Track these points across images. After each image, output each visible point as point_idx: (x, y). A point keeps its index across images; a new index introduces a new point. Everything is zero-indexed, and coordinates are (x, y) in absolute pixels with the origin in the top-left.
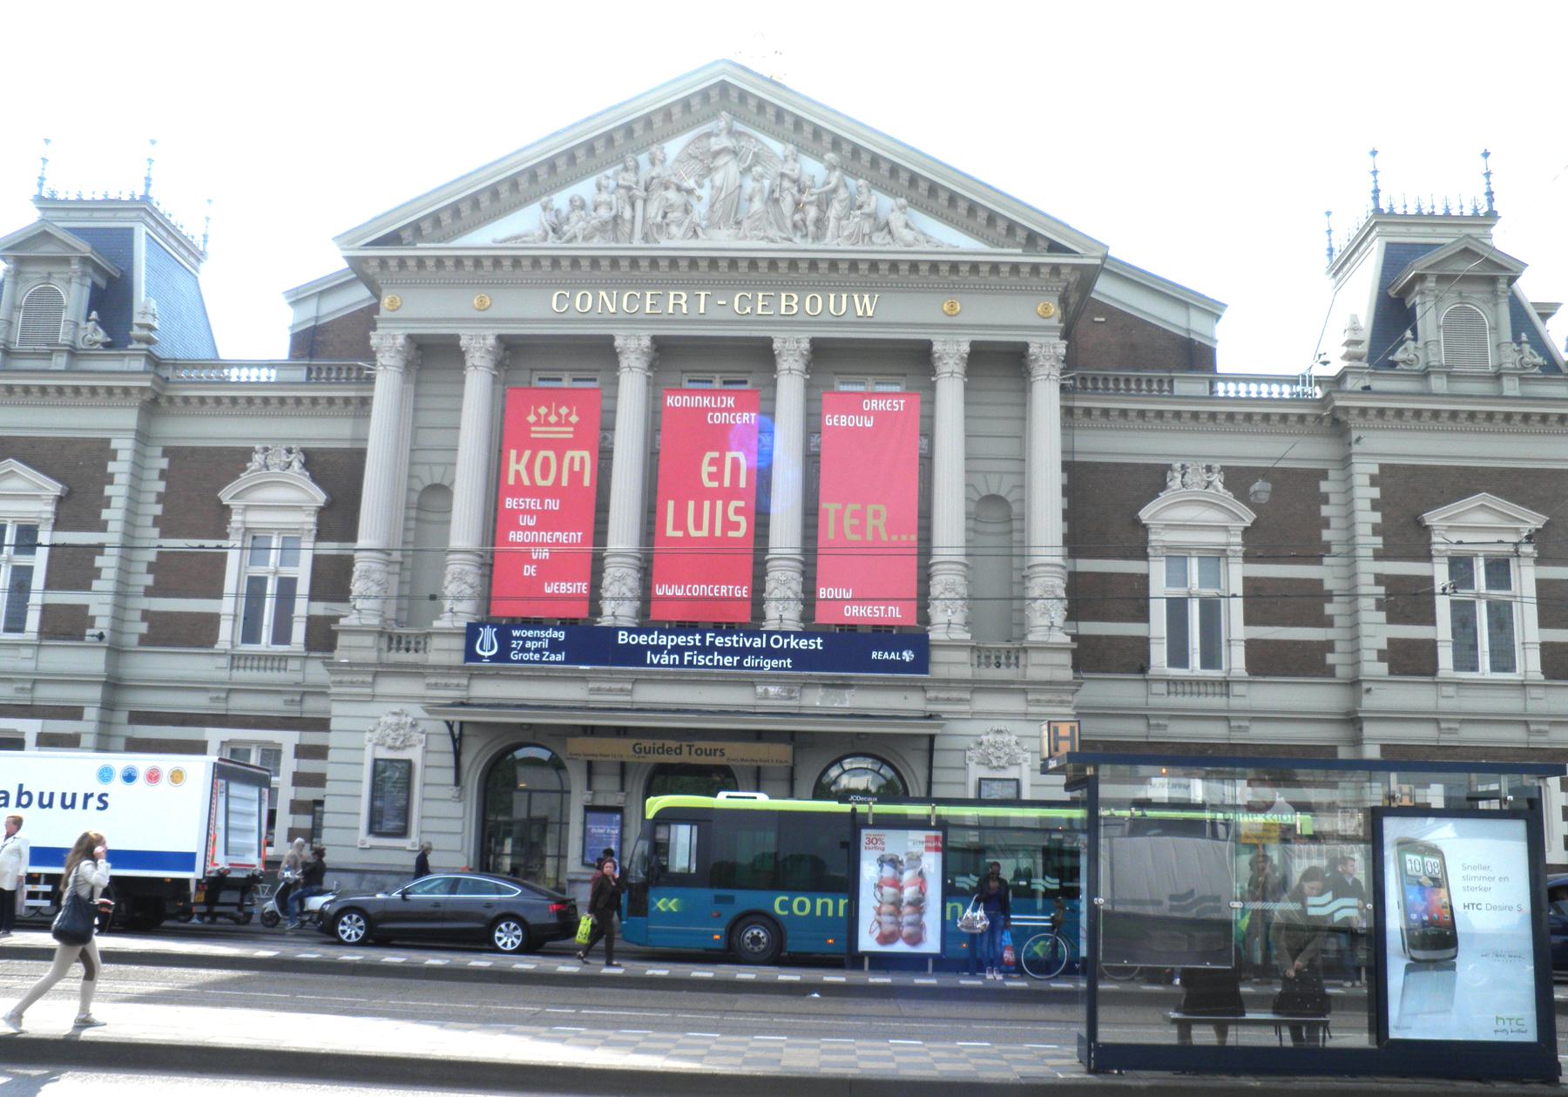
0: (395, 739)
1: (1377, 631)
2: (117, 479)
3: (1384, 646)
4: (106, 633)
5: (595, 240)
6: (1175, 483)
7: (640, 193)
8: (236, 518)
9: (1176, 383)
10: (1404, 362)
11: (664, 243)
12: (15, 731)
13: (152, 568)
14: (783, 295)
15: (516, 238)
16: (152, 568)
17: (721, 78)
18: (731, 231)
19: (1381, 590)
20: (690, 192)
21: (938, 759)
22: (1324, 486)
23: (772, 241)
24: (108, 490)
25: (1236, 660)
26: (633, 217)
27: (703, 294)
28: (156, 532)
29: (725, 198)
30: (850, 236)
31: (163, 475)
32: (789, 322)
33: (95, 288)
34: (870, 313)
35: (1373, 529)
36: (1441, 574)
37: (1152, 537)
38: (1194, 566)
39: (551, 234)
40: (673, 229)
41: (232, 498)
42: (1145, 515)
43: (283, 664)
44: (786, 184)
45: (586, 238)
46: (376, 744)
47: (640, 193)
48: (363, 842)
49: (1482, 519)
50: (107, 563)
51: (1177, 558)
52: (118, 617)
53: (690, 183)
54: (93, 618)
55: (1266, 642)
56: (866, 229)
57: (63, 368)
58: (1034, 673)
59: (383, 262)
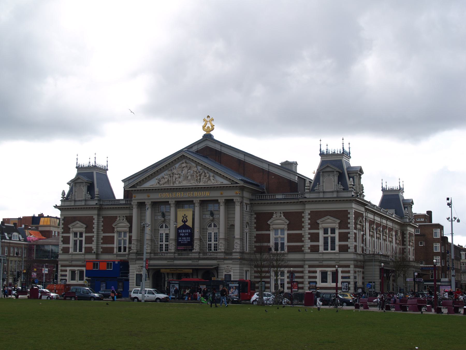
0: (139, 271)
2: (95, 224)
3: (310, 246)
4: (95, 252)
5: (165, 185)
6: (274, 216)
7: (172, 175)
9: (276, 196)
10: (316, 190)
11: (175, 185)
12: (82, 270)
13: (102, 239)
14: (195, 193)
15: (152, 185)
16: (102, 239)
17: (182, 154)
18: (186, 182)
19: (309, 236)
20: (180, 174)
21: (219, 271)
22: (303, 215)
23: (192, 184)
24: (94, 226)
25: (286, 249)
26: (171, 179)
27: (182, 193)
28: (102, 232)
29: (185, 176)
30: (204, 182)
31: (103, 221)
32: (196, 197)
33: (88, 186)
34: (209, 195)
35: (309, 224)
36: (321, 232)
37: (271, 227)
38: (279, 231)
39: (158, 184)
40: (177, 182)
41: (115, 226)
42: (269, 222)
43: (125, 256)
44: (195, 172)
45: (163, 184)
46: (136, 271)
47: (172, 175)
48: (135, 287)
50: (95, 239)
51: (276, 230)
53: (180, 172)
54: (93, 249)
56: (207, 181)
57: (84, 204)
59: (132, 190)
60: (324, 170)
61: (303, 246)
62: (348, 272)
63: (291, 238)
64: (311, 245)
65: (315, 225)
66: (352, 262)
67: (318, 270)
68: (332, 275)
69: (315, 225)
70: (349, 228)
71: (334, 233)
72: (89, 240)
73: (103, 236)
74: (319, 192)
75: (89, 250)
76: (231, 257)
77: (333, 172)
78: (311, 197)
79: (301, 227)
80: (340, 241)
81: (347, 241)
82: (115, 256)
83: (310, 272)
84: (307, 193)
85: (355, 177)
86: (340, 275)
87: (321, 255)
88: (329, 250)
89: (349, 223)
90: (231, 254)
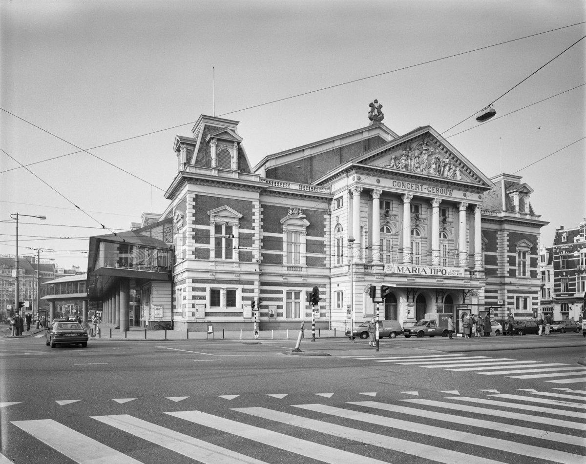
1: (507, 268)
8: (284, 228)
67: (515, 295)
72: (245, 240)
73: (264, 236)
75: (245, 258)
82: (286, 268)
83: (509, 298)
87: (518, 280)
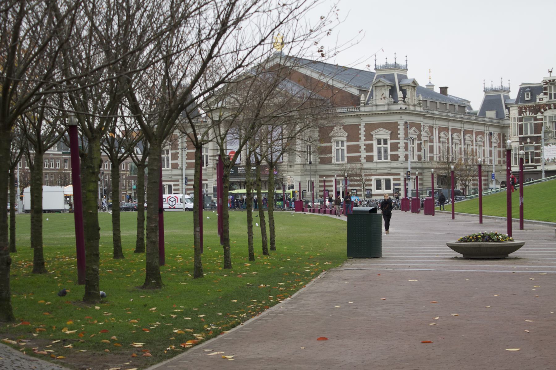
19: (365, 147)
25: (346, 159)
36: (375, 143)
38: (340, 143)
42: (331, 135)
49: (381, 132)
52: (182, 164)
55: (350, 156)
58: (295, 168)
60: (376, 85)
61: (360, 156)
62: (399, 179)
63: (350, 149)
64: (366, 156)
65: (369, 137)
66: (402, 170)
67: (373, 178)
68: (386, 182)
69: (369, 137)
70: (399, 139)
71: (387, 144)
74: (372, 106)
76: (292, 168)
77: (384, 86)
78: (366, 110)
79: (358, 139)
80: (391, 151)
81: (398, 151)
84: (362, 106)
85: (407, 89)
86: (392, 182)
88: (383, 160)
89: (399, 134)
90: (293, 166)
